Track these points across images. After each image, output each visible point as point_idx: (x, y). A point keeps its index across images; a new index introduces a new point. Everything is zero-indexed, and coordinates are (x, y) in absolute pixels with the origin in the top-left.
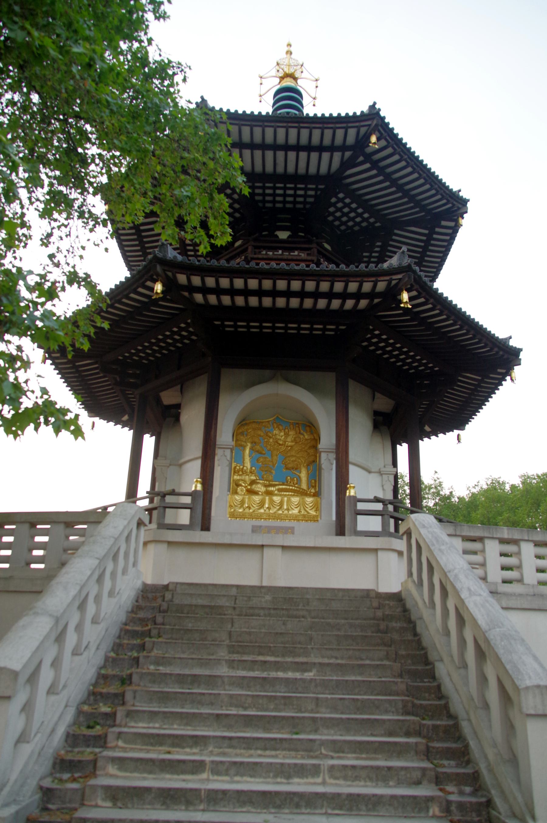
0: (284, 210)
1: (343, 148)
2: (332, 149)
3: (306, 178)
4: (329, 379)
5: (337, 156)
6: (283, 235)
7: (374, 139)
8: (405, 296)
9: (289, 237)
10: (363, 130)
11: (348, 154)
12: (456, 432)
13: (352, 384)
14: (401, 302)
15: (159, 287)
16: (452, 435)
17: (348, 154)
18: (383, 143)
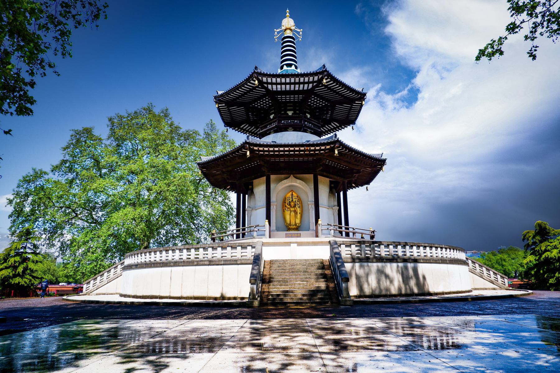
0: (290, 102)
1: (313, 82)
2: (308, 83)
3: (299, 92)
4: (311, 176)
5: (311, 85)
6: (290, 113)
7: (325, 81)
8: (336, 152)
9: (293, 114)
10: (320, 76)
11: (315, 84)
12: (366, 186)
13: (320, 177)
14: (335, 153)
15: (248, 153)
16: (365, 186)
17: (315, 84)
18: (329, 80)
